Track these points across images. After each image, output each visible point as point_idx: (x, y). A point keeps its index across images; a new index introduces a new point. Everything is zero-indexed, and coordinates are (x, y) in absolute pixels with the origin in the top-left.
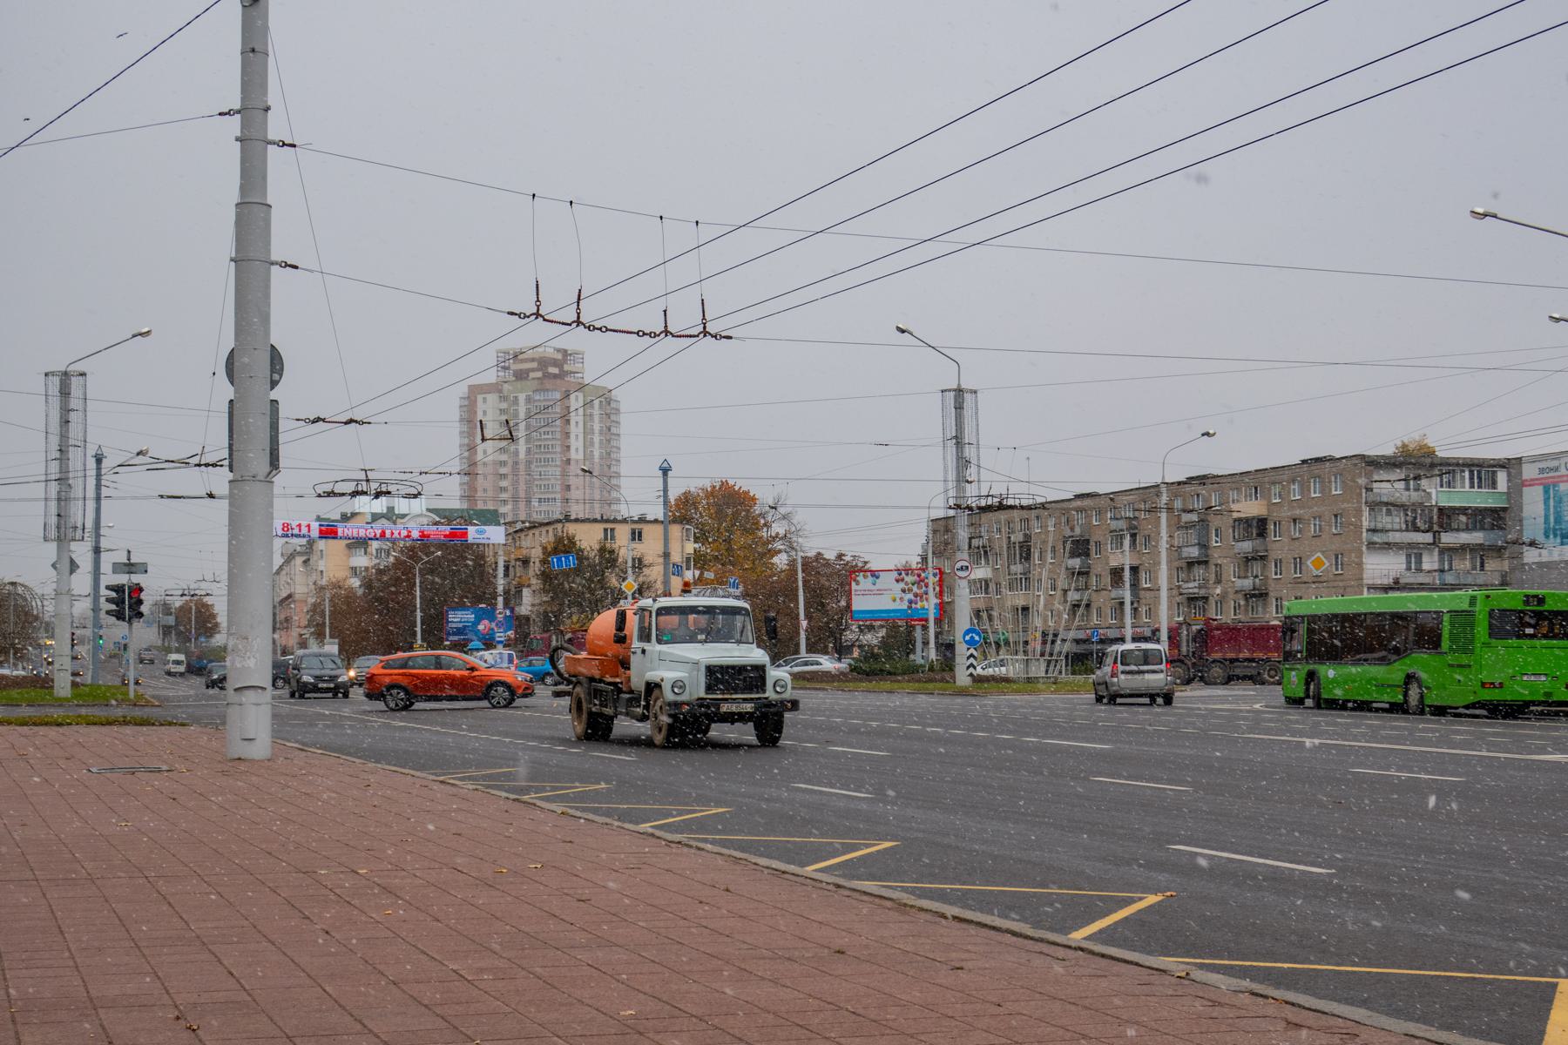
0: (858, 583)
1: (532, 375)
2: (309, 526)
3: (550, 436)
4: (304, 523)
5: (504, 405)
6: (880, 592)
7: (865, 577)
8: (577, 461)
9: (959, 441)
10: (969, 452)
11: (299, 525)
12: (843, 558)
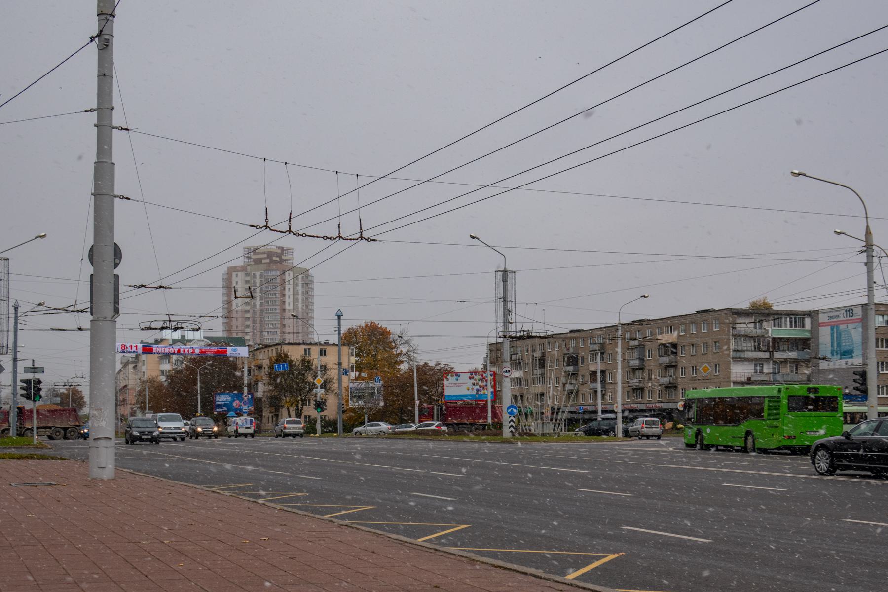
0: (448, 380)
1: (264, 261)
2: (136, 346)
3: (274, 296)
4: (134, 345)
5: (248, 279)
6: (460, 385)
7: (452, 376)
8: (289, 310)
9: (505, 300)
10: (510, 306)
11: (131, 346)
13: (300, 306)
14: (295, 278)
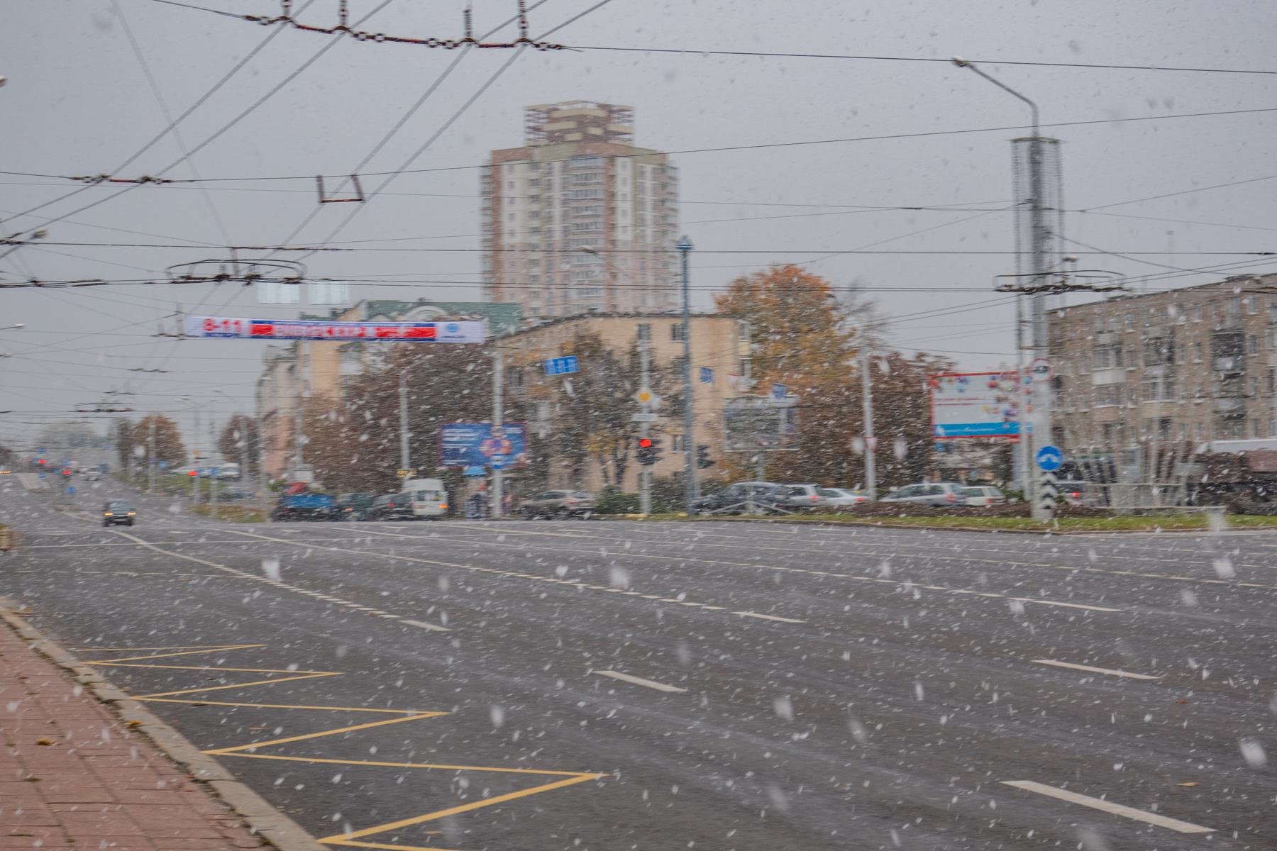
1: (570, 137)
6: (969, 402)
9: (1036, 206)
10: (1050, 219)
12: (923, 358)
13: (649, 231)
14: (639, 174)
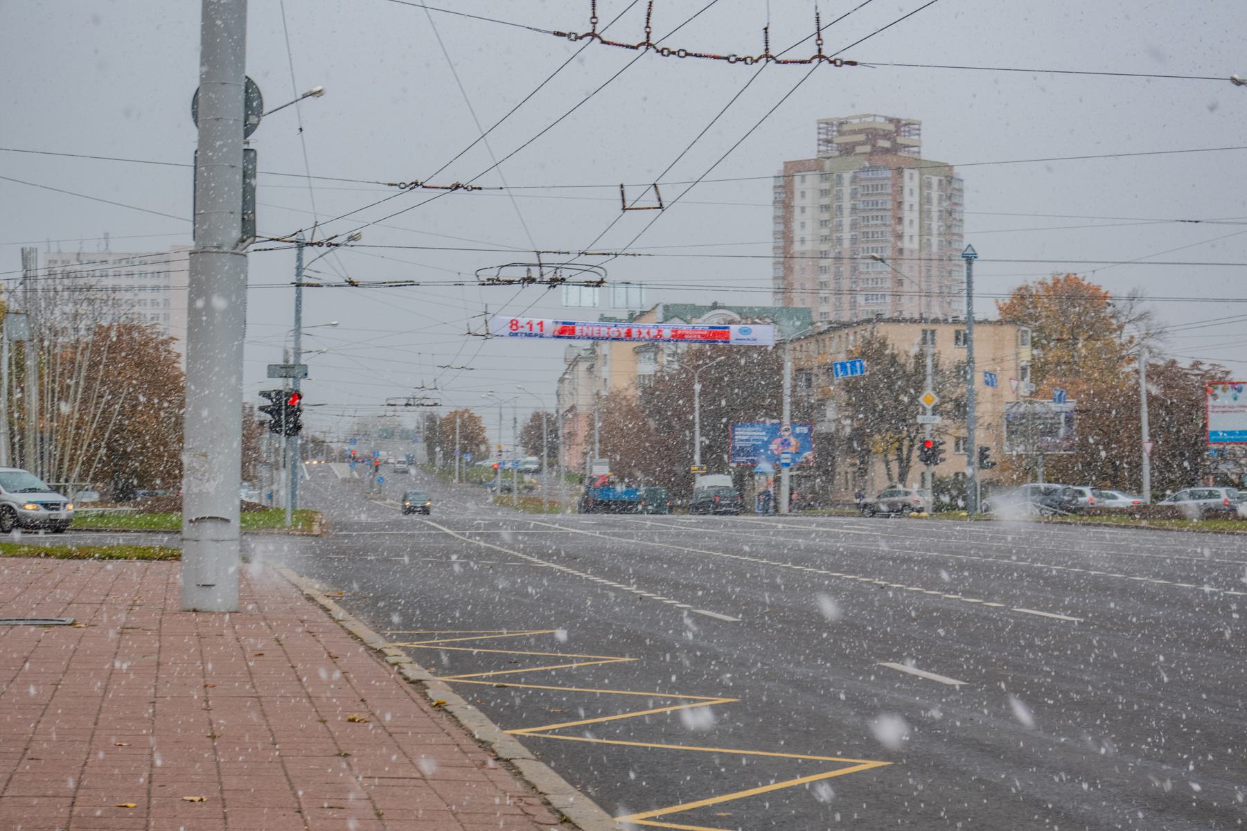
0: (1215, 397)
1: (859, 149)
2: (541, 324)
3: (879, 222)
4: (536, 321)
5: (826, 186)
7: (1224, 390)
8: (911, 251)
11: (541, 324)
12: (1200, 367)
13: (935, 241)
14: (925, 185)
